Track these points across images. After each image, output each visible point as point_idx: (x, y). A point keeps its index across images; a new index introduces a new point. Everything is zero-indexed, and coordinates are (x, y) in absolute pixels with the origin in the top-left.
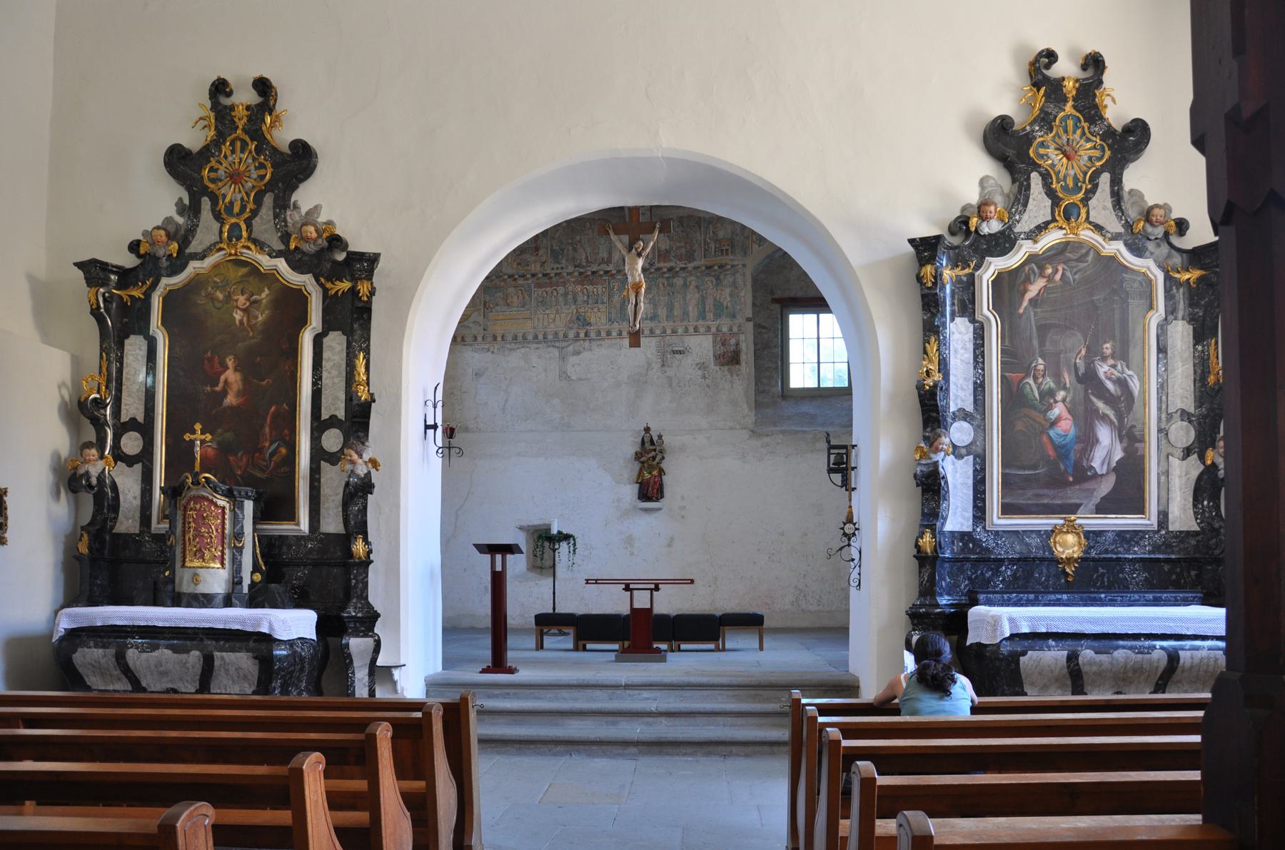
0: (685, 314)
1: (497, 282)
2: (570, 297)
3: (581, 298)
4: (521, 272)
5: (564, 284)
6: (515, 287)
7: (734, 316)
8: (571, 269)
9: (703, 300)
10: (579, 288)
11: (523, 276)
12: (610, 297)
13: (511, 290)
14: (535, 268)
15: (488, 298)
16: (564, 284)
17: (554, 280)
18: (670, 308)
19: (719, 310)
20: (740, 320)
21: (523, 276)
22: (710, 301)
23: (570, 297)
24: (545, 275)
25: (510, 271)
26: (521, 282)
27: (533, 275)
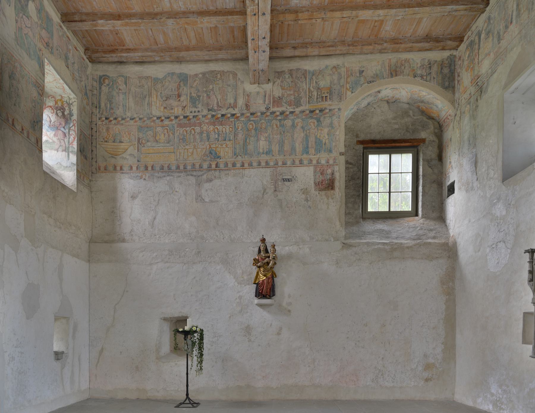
0: (293, 149)
1: (148, 122)
2: (205, 135)
3: (213, 136)
4: (167, 115)
5: (200, 125)
6: (163, 127)
7: (330, 151)
8: (205, 112)
9: (307, 137)
10: (212, 128)
11: (168, 118)
12: (235, 135)
13: (159, 129)
14: (178, 111)
15: (141, 135)
16: (200, 125)
17: (193, 121)
18: (282, 144)
19: (319, 146)
20: (335, 154)
21: (168, 118)
22: (312, 139)
23: (205, 135)
24: (185, 117)
25: (158, 114)
26: (166, 122)
27: (176, 117)
